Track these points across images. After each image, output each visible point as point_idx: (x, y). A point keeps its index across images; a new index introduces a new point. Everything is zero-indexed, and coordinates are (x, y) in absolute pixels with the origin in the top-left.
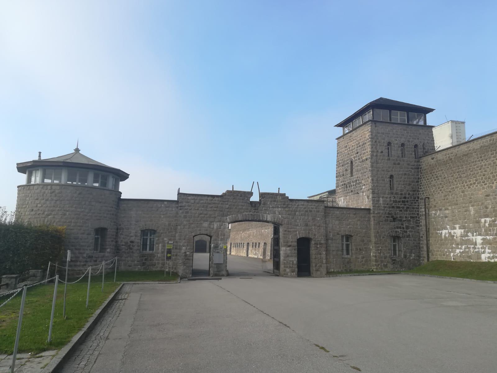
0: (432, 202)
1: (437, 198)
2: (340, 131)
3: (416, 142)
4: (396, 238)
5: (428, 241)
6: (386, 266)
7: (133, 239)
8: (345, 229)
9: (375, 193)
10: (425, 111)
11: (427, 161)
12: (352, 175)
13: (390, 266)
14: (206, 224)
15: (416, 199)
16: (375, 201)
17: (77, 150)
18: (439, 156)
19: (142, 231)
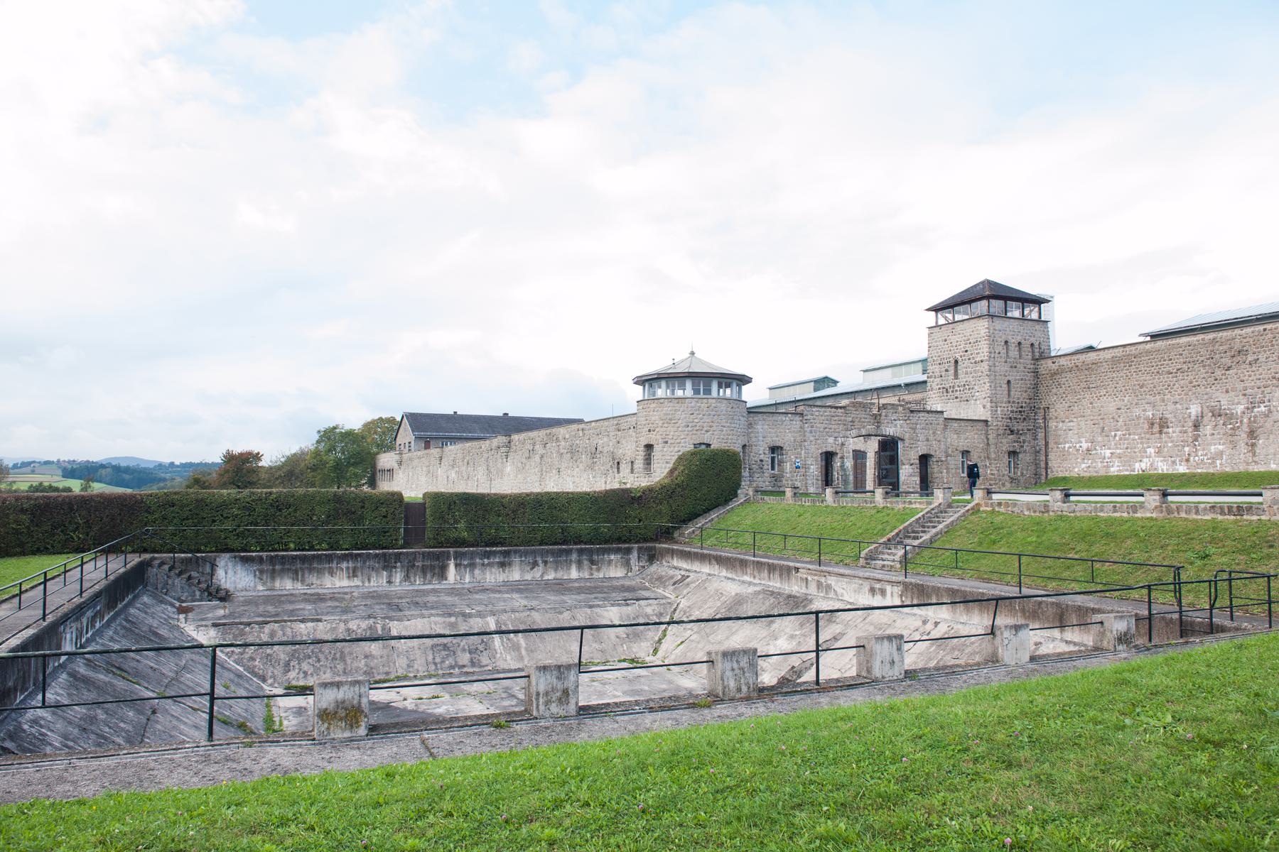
0: (1052, 413)
1: (1059, 409)
2: (931, 318)
3: (1032, 340)
4: (1013, 454)
5: (1047, 456)
6: (1003, 485)
7: (762, 457)
8: (963, 444)
9: (994, 402)
10: (1038, 301)
11: (1047, 366)
12: (956, 375)
13: (1008, 485)
14: (831, 440)
15: (1034, 409)
16: (994, 412)
17: (693, 353)
18: (1063, 361)
19: (427, 446)
